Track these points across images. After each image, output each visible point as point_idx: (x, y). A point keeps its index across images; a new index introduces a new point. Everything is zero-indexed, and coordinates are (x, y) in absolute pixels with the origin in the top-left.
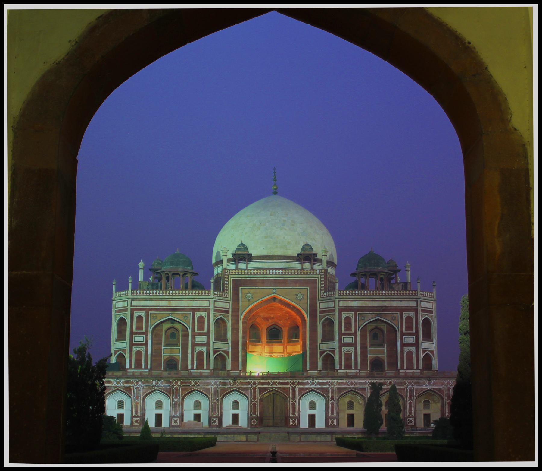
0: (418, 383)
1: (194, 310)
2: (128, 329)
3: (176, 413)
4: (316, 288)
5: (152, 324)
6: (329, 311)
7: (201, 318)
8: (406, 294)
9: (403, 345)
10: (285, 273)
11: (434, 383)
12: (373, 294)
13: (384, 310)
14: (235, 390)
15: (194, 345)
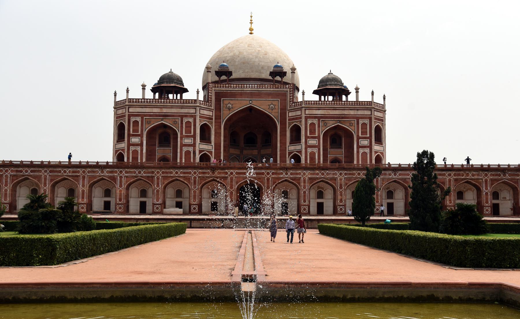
0: (385, 174)
1: (182, 117)
2: (126, 132)
3: (158, 200)
4: (286, 100)
5: (146, 127)
6: (297, 119)
7: (188, 123)
8: (362, 104)
9: (359, 147)
10: (260, 87)
11: (400, 175)
12: (334, 104)
13: (343, 118)
14: (214, 180)
15: (182, 145)
